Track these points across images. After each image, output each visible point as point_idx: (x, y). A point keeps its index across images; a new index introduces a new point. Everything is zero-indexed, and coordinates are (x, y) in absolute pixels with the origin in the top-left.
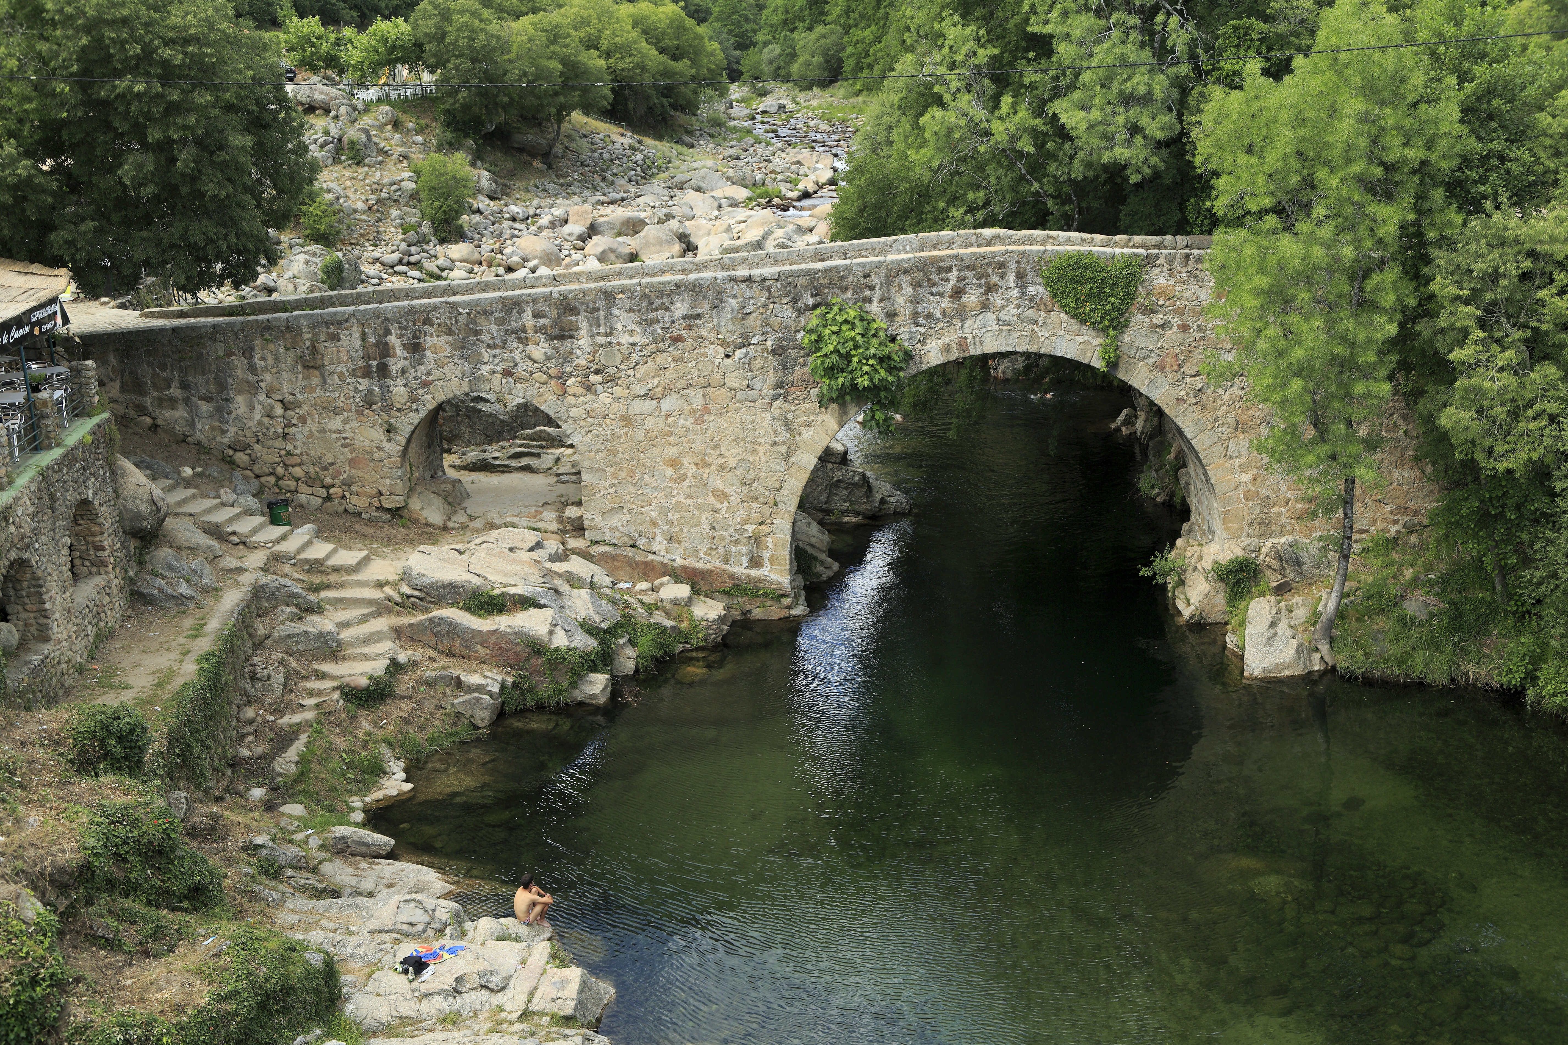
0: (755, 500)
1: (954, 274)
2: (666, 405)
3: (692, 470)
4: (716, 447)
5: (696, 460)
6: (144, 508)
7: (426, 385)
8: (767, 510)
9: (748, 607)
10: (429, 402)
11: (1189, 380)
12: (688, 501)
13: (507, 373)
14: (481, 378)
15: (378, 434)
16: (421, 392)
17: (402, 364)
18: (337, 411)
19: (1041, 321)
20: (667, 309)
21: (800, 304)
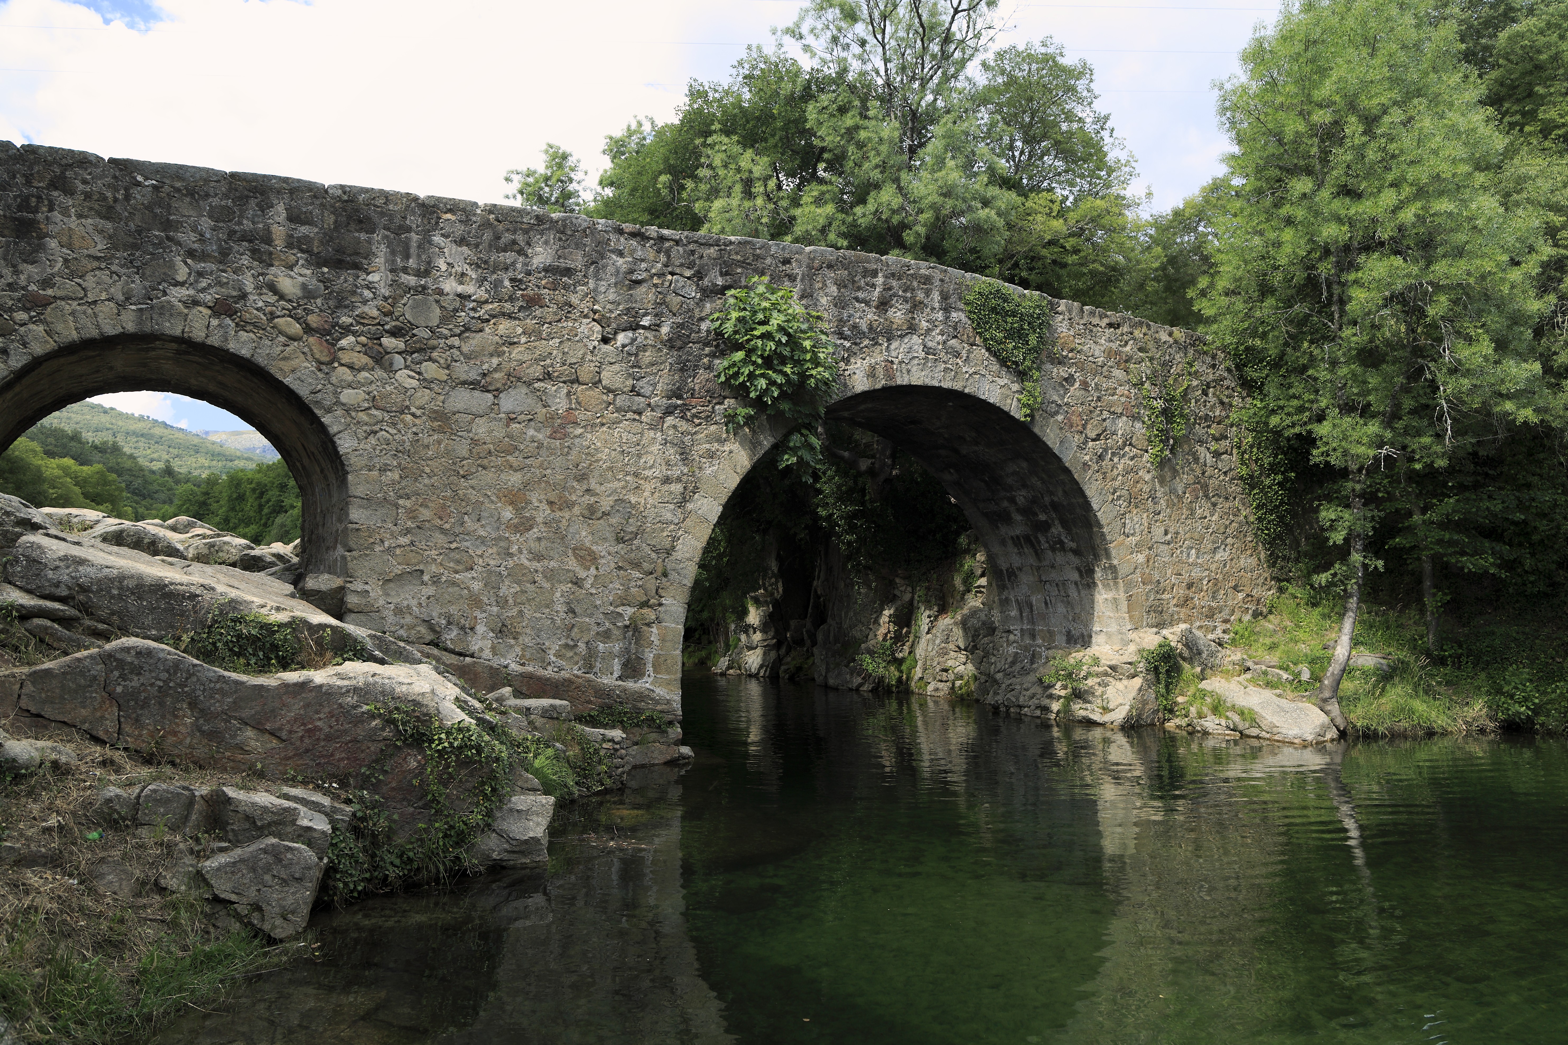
0: (637, 565)
1: (880, 280)
2: (509, 402)
3: (543, 513)
4: (582, 478)
5: (553, 496)
8: (651, 583)
11: (1091, 444)
12: (536, 565)
14: (166, 310)
16: (21, 316)
19: (964, 354)
20: (521, 252)
21: (706, 282)
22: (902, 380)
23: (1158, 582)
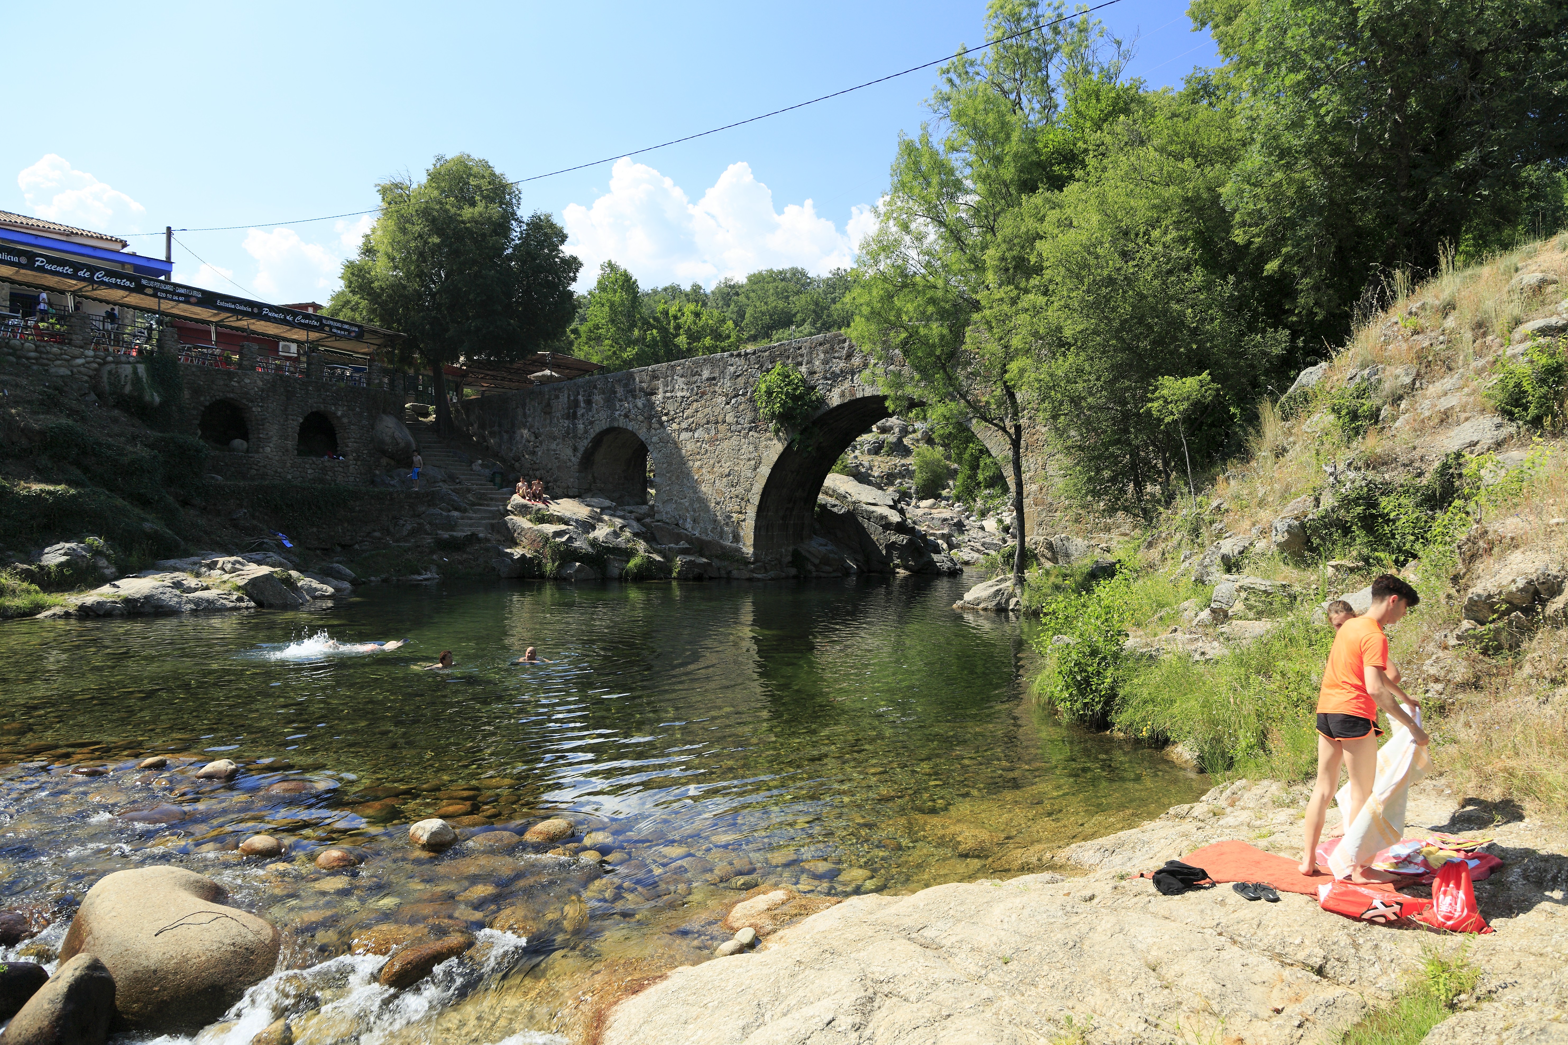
6: (388, 439)
7: (591, 423)
9: (730, 569)
10: (592, 433)
13: (626, 416)
14: (614, 419)
15: (569, 452)
17: (583, 411)
18: (555, 438)
22: (859, 395)
23: (1051, 504)
